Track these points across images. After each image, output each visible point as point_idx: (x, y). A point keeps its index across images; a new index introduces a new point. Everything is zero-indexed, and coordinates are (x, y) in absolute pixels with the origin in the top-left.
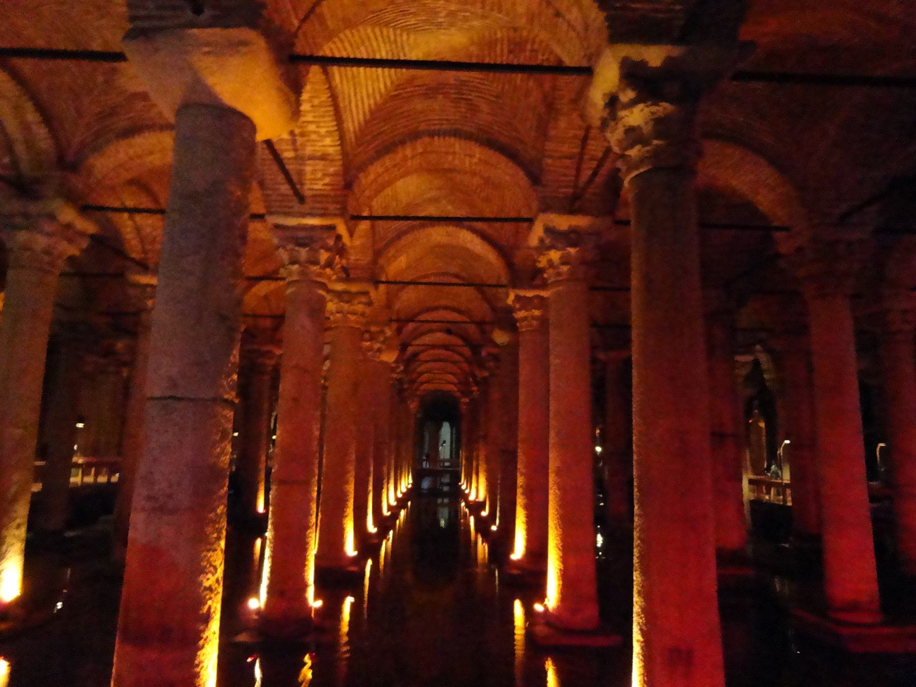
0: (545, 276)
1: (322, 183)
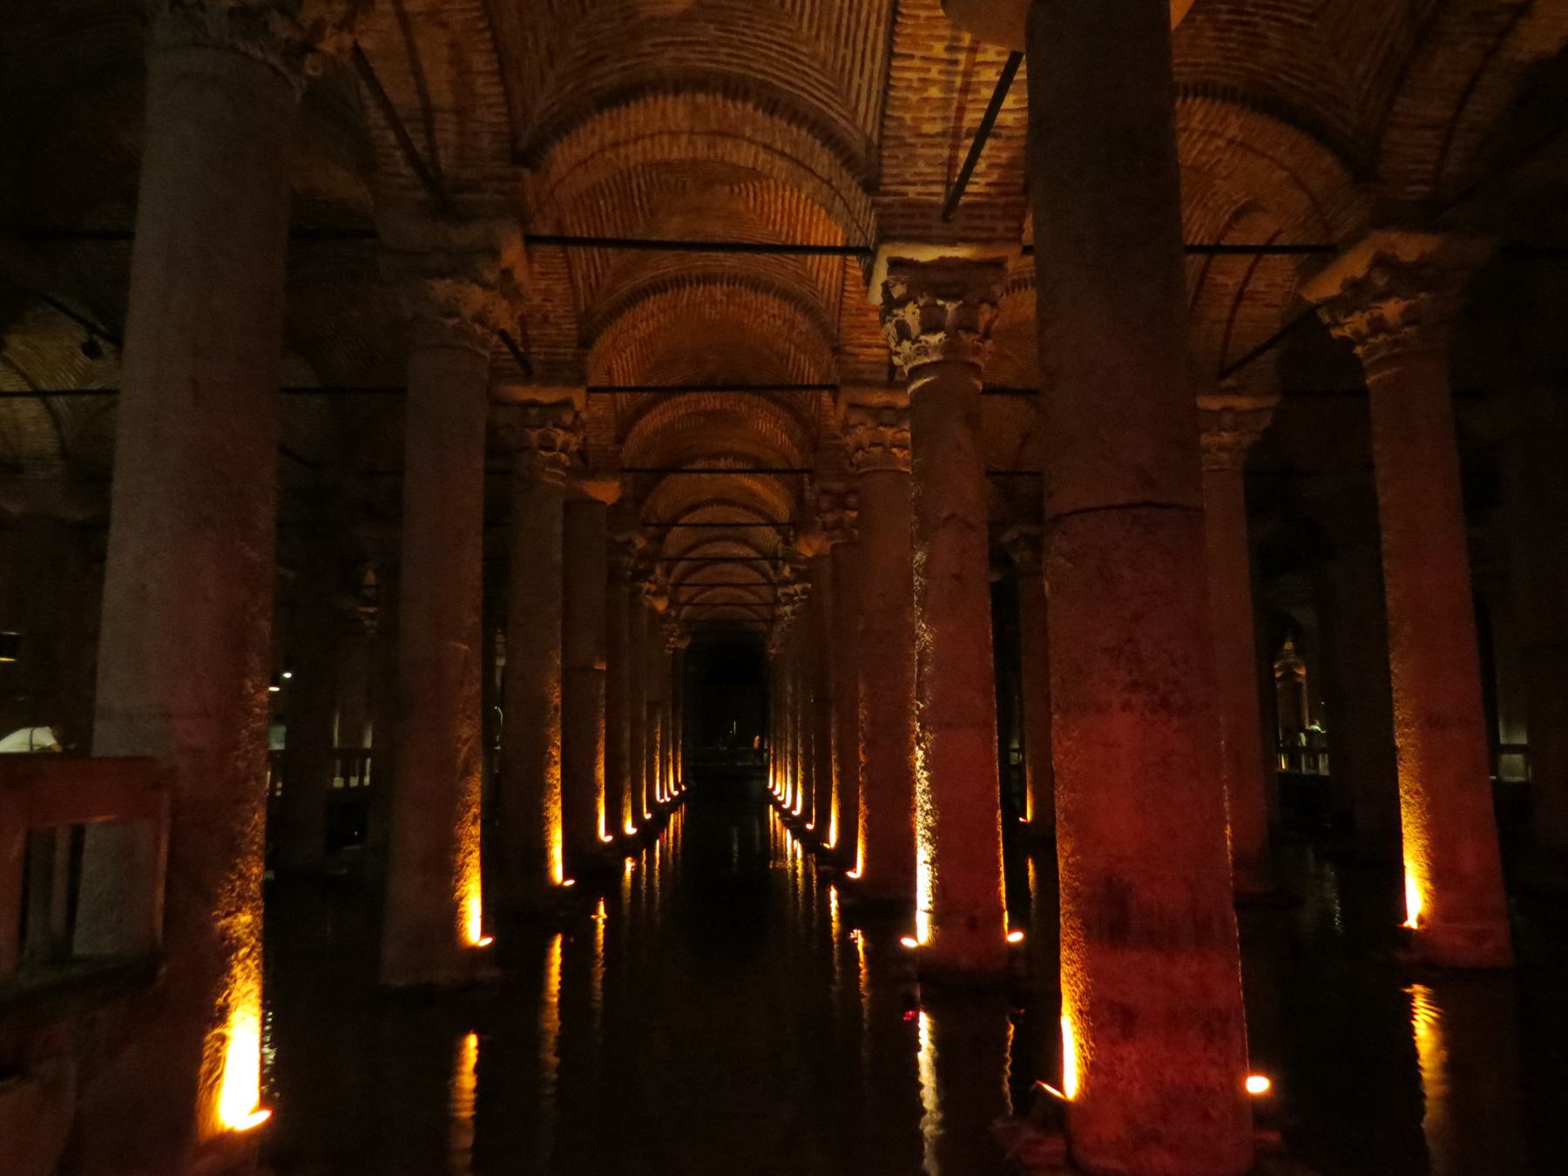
0: (1359, 350)
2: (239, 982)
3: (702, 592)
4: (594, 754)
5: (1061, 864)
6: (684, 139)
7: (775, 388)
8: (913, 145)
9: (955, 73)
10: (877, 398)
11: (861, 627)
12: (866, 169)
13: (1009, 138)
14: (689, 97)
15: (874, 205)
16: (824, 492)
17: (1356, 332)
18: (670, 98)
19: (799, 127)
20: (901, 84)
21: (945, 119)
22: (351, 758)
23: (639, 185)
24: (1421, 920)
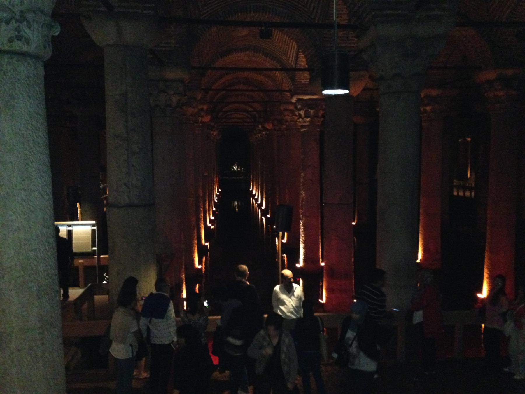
24: (420, 260)
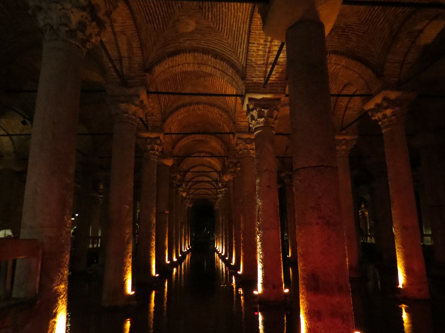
0: (380, 123)
1: (274, 77)
2: (60, 305)
3: (196, 191)
4: (165, 237)
5: (299, 269)
6: (191, 65)
7: (216, 133)
8: (255, 67)
9: (266, 48)
10: (246, 136)
11: (241, 201)
12: (242, 73)
13: (282, 65)
14: (193, 54)
15: (244, 83)
16: (231, 162)
17: (379, 118)
18: (188, 54)
19: (223, 62)
20: (252, 51)
21: (264, 60)
22: (95, 239)
23: (179, 78)
24: (403, 285)
